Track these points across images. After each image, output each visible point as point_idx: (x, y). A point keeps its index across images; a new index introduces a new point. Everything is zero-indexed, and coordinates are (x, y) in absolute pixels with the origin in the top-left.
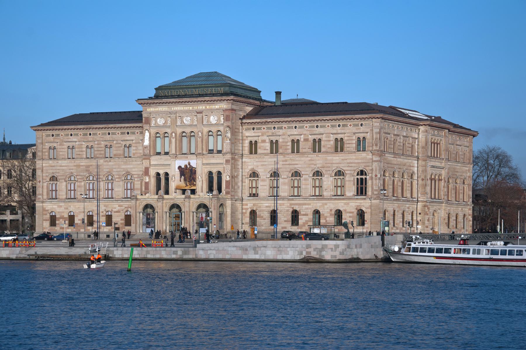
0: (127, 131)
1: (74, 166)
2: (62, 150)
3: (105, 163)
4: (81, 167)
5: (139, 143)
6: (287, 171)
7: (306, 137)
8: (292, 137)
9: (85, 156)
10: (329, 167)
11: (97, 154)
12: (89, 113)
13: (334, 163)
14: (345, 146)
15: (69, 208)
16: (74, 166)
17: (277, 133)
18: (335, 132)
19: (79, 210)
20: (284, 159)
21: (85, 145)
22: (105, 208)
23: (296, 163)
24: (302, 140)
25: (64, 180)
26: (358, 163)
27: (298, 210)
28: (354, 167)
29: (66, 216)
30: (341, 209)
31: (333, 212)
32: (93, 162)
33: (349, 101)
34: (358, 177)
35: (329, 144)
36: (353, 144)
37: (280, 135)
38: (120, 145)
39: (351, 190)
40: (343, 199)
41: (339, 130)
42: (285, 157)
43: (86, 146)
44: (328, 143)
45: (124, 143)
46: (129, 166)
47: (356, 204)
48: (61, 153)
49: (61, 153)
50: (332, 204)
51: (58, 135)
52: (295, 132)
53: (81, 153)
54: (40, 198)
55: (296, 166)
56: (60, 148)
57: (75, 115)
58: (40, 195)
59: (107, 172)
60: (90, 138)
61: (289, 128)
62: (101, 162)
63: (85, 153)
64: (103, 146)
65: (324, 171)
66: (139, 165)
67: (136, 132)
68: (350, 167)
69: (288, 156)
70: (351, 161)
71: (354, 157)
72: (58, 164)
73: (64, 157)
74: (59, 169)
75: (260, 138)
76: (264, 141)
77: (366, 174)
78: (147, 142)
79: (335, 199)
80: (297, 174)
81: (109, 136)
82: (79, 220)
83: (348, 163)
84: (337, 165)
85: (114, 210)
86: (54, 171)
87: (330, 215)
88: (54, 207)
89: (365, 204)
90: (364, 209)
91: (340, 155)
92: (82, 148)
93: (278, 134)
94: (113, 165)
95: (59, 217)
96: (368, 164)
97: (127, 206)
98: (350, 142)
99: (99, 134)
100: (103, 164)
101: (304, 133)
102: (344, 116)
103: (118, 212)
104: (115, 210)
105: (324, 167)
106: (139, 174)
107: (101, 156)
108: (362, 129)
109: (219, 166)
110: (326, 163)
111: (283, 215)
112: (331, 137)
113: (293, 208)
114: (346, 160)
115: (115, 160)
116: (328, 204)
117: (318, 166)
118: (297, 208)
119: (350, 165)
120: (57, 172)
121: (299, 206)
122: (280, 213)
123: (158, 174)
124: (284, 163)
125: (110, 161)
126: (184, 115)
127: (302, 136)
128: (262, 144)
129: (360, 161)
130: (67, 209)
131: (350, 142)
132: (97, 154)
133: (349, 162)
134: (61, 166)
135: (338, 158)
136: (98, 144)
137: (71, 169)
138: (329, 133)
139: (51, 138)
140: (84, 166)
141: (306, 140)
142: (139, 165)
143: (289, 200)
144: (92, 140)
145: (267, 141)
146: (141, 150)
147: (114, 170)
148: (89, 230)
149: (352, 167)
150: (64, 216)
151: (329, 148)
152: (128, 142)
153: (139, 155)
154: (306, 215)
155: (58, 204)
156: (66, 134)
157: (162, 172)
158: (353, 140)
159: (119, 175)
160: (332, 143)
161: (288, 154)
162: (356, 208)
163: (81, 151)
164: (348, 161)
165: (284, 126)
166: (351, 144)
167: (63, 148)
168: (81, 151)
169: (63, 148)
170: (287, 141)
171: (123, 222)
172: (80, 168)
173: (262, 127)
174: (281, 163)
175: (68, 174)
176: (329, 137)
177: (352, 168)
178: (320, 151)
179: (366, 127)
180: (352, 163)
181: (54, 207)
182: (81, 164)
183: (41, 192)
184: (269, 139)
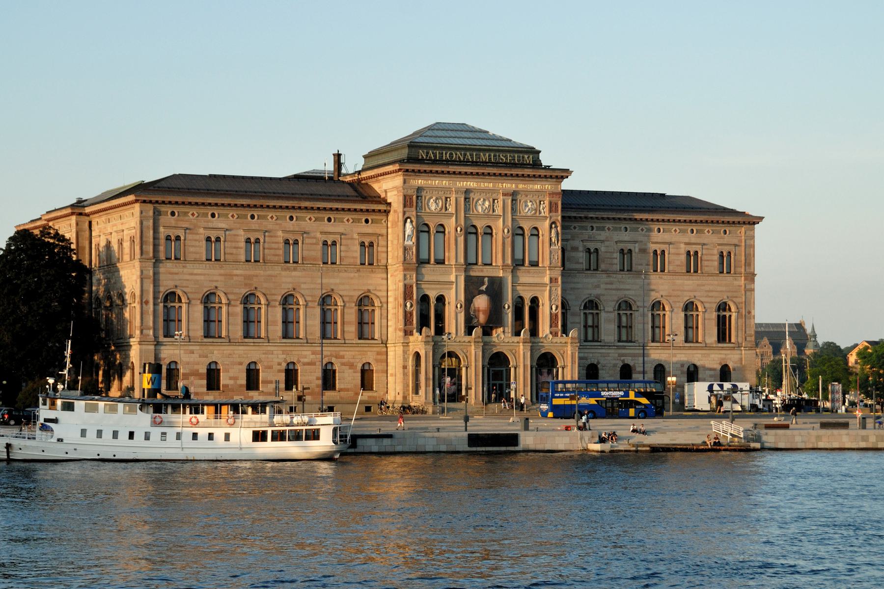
0: (328, 216)
1: (221, 275)
2: (194, 243)
3: (284, 273)
4: (235, 278)
5: (352, 239)
6: (614, 301)
7: (643, 247)
8: (621, 246)
9: (243, 258)
10: (679, 296)
11: (269, 255)
12: (207, 173)
13: (685, 291)
15: (209, 355)
16: (221, 275)
17: (596, 237)
18: (687, 240)
19: (232, 359)
20: (608, 280)
21: (242, 236)
22: (284, 356)
23: (628, 287)
24: (637, 250)
25: (199, 301)
26: (721, 291)
27: (631, 364)
28: (716, 297)
30: (698, 363)
31: (685, 369)
32: (259, 271)
33: (669, 193)
34: (719, 313)
35: (678, 260)
36: (712, 261)
37: (602, 241)
38: (314, 241)
39: (708, 331)
40: (701, 348)
41: (693, 238)
42: (609, 276)
43: (246, 237)
45: (324, 237)
46: (332, 281)
47: (720, 356)
48: (192, 249)
49: (192, 249)
50: (683, 355)
52: (625, 236)
53: (234, 251)
54: (148, 335)
55: (627, 292)
56: (190, 240)
57: (174, 177)
58: (149, 329)
59: (288, 289)
60: (255, 224)
61: (615, 229)
62: (277, 270)
63: (243, 251)
64: (281, 240)
66: (352, 278)
67: (346, 219)
68: (710, 297)
69: (615, 276)
70: (711, 288)
71: (716, 282)
72: (185, 270)
73: (198, 256)
74: (188, 280)
75: (568, 243)
79: (690, 348)
80: (626, 305)
81: (292, 222)
82: (231, 378)
83: (706, 291)
84: (692, 294)
85: (302, 360)
86: (177, 283)
87: (681, 374)
88: (177, 352)
89: (732, 356)
91: (694, 278)
92: (238, 242)
93: (598, 238)
94: (299, 277)
95: (188, 372)
96: (735, 294)
97: (329, 353)
98: (709, 258)
99: (272, 217)
100: (280, 274)
101: (640, 240)
102: (708, 217)
103: (311, 363)
104: (306, 360)
105: (671, 296)
106: (352, 296)
107: (276, 258)
108: (727, 239)
109: (538, 288)
110: (673, 290)
111: (608, 373)
112: (680, 248)
113: (623, 361)
114: (704, 285)
115: (305, 268)
116: (678, 355)
117: (662, 293)
118: (629, 361)
119: (710, 294)
120: (184, 285)
121: (634, 358)
122: (603, 369)
124: (609, 286)
125: (295, 269)
127: (637, 245)
128: (574, 254)
129: (724, 289)
130: (207, 357)
131: (709, 258)
132: (269, 255)
133: (708, 289)
134: (192, 274)
135: (691, 282)
136: (269, 236)
137: (210, 281)
138: (680, 243)
140: (241, 275)
142: (352, 278)
143: (619, 347)
144: (258, 228)
145: (581, 249)
146: (356, 251)
147: (303, 286)
148: (252, 397)
149: (712, 297)
150: (198, 371)
151: (677, 266)
152: (331, 236)
153: (352, 261)
155: (186, 348)
156: (203, 213)
157: (433, 295)
158: (714, 255)
159: (312, 296)
160: (683, 257)
161: (615, 272)
162: (718, 362)
163: (235, 248)
164: (707, 288)
165: (607, 226)
166: (711, 262)
167: (196, 240)
168: (235, 248)
169: (196, 240)
170: (613, 251)
171: (320, 382)
172: (233, 279)
173: (571, 226)
174: (602, 286)
175: (205, 290)
176: (677, 248)
177: (713, 300)
178: (663, 270)
179: (733, 236)
180: (712, 291)
181: (177, 352)
183: (151, 324)
184: (585, 246)
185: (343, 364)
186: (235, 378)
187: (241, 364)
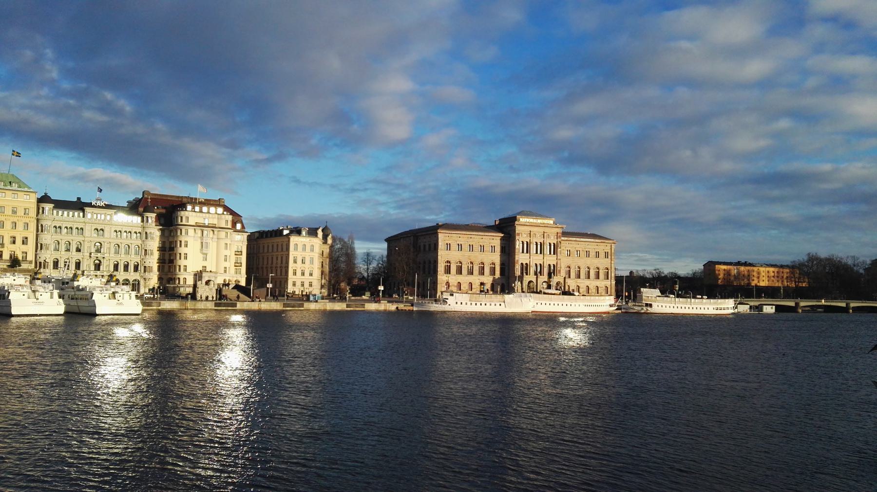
8: (576, 249)
14: (600, 255)
29: (456, 284)
30: (598, 286)
31: (595, 287)
44: (592, 254)
51: (452, 237)
65: (590, 267)
76: (563, 250)
77: (608, 269)
78: (517, 247)
90: (608, 286)
123: (522, 264)
125: (483, 254)
126: (537, 233)
139: (448, 238)
141: (583, 251)
154: (582, 288)
157: (524, 263)
166: (602, 255)
182: (466, 255)
185: (496, 284)
186: (465, 287)
187: (466, 283)
